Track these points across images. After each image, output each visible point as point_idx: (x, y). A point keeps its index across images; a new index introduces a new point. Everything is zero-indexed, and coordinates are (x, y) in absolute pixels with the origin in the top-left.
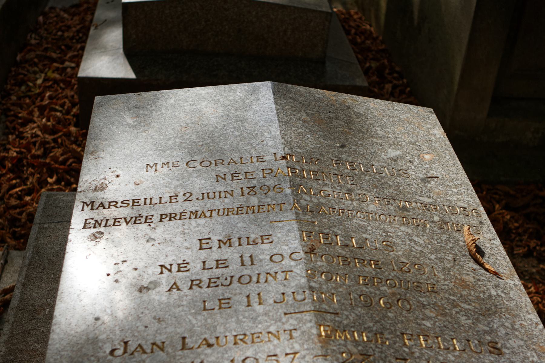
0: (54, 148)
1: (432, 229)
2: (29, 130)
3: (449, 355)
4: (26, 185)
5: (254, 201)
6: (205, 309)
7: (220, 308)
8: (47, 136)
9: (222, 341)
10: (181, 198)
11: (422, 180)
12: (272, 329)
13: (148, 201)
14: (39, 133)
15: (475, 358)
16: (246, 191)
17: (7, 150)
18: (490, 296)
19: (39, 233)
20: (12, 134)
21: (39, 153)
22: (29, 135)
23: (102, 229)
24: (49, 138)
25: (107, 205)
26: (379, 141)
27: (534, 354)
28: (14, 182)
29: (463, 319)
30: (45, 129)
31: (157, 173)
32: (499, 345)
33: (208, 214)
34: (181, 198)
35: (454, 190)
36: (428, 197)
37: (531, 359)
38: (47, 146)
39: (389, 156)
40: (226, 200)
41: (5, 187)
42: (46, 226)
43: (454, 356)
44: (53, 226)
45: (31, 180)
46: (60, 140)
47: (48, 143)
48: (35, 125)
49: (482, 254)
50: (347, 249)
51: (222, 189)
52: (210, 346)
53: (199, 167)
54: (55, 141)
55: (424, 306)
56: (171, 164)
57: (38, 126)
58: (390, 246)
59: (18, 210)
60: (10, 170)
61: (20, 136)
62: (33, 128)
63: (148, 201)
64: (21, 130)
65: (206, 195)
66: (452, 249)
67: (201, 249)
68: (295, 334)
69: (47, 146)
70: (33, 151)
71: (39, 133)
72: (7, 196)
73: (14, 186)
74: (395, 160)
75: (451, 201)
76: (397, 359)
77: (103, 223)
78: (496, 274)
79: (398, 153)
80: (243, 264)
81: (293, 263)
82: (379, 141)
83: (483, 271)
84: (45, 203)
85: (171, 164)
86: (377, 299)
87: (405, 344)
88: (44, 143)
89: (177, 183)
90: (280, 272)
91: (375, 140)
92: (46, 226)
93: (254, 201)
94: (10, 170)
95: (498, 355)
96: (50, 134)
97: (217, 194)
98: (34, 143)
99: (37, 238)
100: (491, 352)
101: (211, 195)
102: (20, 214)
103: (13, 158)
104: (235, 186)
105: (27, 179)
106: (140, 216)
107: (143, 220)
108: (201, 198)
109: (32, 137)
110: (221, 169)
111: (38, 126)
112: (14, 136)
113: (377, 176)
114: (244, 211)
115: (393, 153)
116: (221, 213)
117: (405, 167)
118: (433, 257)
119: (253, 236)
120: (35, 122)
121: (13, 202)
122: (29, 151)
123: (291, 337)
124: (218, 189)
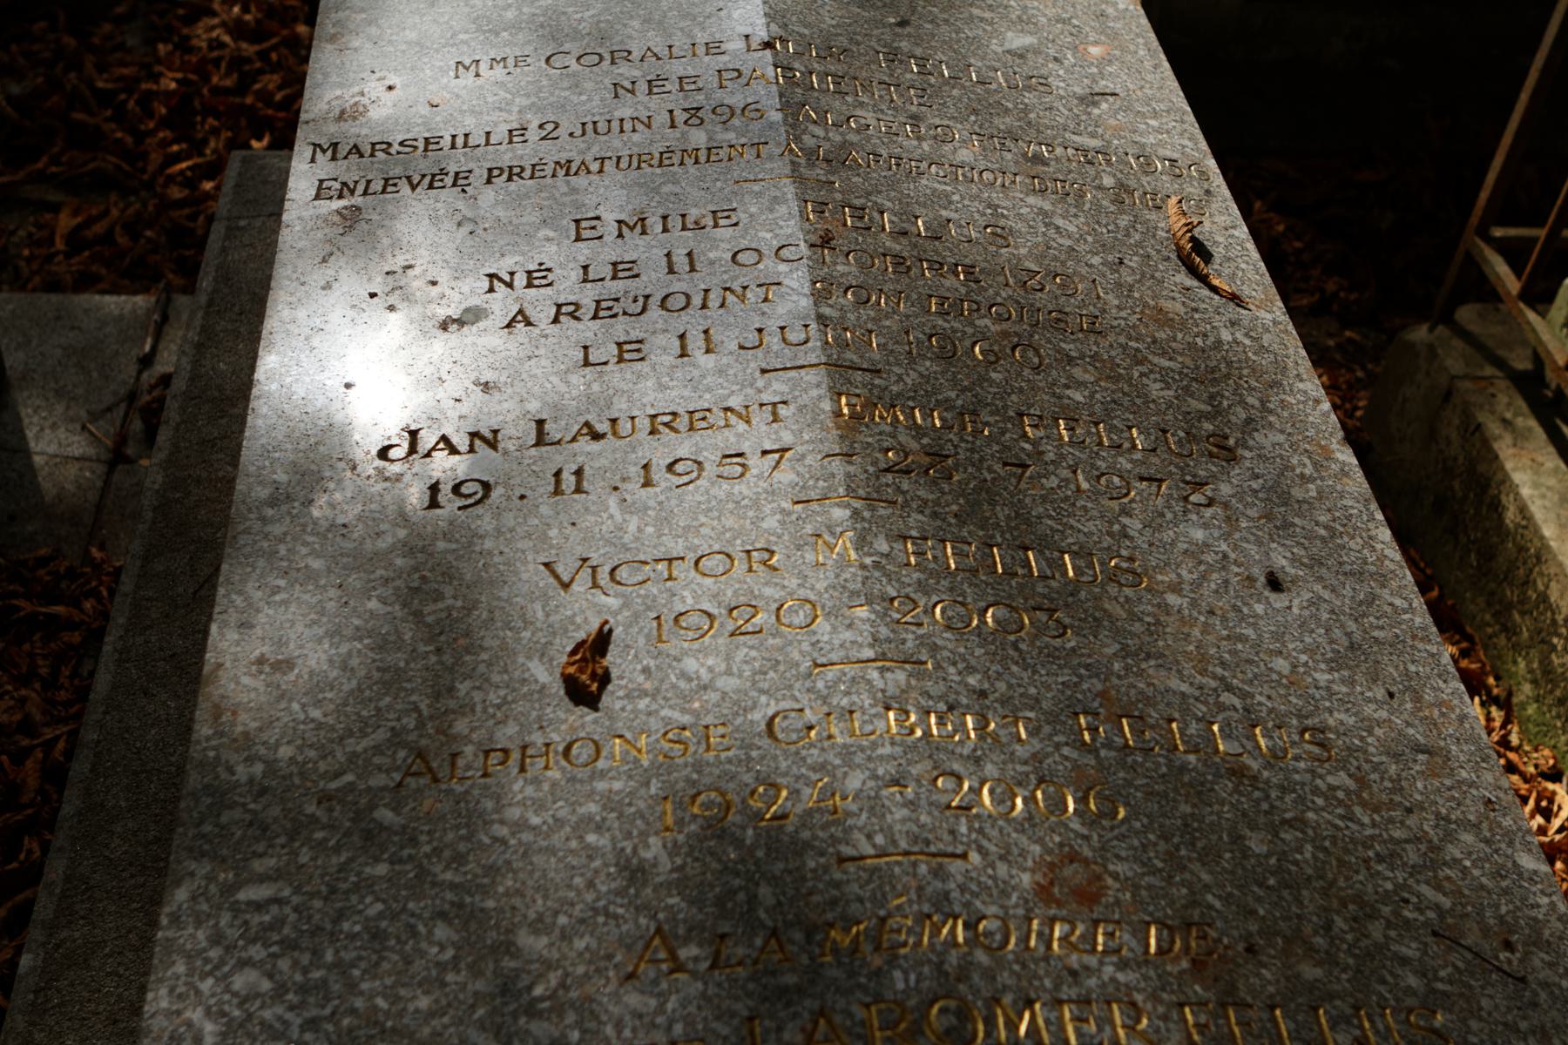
0: (261, 72)
1: (1096, 203)
2: (204, 33)
3: (1120, 459)
4: (201, 154)
5: (698, 138)
6: (587, 363)
7: (621, 360)
8: (244, 45)
9: (625, 427)
10: (533, 134)
11: (1082, 99)
12: (733, 402)
13: (460, 141)
14: (227, 39)
15: (1177, 466)
16: (680, 117)
17: (156, 78)
18: (1219, 343)
19: (227, 237)
20: (166, 41)
21: (228, 83)
22: (204, 45)
23: (357, 200)
24: (249, 49)
25: (367, 150)
26: (988, 15)
27: (1307, 461)
28: (175, 148)
29: (1155, 389)
30: (238, 30)
31: (480, 81)
32: (1231, 442)
33: (595, 167)
34: (533, 134)
35: (1153, 122)
36: (1093, 135)
37: (1298, 471)
38: (247, 68)
39: (1007, 46)
40: (636, 137)
41: (156, 158)
42: (242, 223)
43: (1131, 461)
44: (258, 223)
45: (212, 144)
46: (274, 56)
47: (248, 60)
48: (216, 21)
49: (1207, 257)
50: (904, 241)
51: (627, 113)
52: (597, 436)
53: (574, 66)
54: (263, 55)
55: (1070, 360)
56: (510, 61)
57: (224, 24)
58: (1002, 236)
59: (186, 211)
60: (164, 123)
61: (184, 46)
62: (213, 28)
63: (460, 141)
64: (185, 31)
65: (589, 127)
66: (1139, 245)
67: (578, 239)
68: (783, 411)
69: (247, 68)
70: (215, 80)
71: (227, 39)
72: (161, 180)
73: (178, 158)
74: (1021, 56)
75: (1143, 146)
76: (1005, 464)
77: (360, 188)
78: (1235, 298)
79: (1028, 40)
80: (671, 271)
81: (783, 267)
82: (988, 15)
83: (1206, 292)
84: (240, 174)
85: (510, 61)
86: (968, 343)
87: (1025, 435)
88: (237, 62)
89: (525, 102)
90: (753, 287)
91: (976, 11)
92: (242, 223)
93: (698, 138)
94: (164, 123)
95: (1228, 461)
96: (252, 41)
97: (615, 125)
98: (217, 62)
99: (224, 250)
100: (1211, 455)
101: (602, 127)
102: (193, 217)
103: (169, 94)
104: (657, 106)
105: (205, 142)
106: (445, 173)
107: (449, 180)
108: (578, 132)
109: (211, 48)
110: (625, 71)
111: (224, 24)
112: (170, 47)
113: (979, 89)
114: (676, 159)
115: (1017, 41)
116: (623, 164)
117: (1044, 72)
118: (1096, 260)
119: (694, 213)
120: (214, 14)
121: (176, 193)
122: (206, 78)
123: (776, 418)
124: (618, 114)
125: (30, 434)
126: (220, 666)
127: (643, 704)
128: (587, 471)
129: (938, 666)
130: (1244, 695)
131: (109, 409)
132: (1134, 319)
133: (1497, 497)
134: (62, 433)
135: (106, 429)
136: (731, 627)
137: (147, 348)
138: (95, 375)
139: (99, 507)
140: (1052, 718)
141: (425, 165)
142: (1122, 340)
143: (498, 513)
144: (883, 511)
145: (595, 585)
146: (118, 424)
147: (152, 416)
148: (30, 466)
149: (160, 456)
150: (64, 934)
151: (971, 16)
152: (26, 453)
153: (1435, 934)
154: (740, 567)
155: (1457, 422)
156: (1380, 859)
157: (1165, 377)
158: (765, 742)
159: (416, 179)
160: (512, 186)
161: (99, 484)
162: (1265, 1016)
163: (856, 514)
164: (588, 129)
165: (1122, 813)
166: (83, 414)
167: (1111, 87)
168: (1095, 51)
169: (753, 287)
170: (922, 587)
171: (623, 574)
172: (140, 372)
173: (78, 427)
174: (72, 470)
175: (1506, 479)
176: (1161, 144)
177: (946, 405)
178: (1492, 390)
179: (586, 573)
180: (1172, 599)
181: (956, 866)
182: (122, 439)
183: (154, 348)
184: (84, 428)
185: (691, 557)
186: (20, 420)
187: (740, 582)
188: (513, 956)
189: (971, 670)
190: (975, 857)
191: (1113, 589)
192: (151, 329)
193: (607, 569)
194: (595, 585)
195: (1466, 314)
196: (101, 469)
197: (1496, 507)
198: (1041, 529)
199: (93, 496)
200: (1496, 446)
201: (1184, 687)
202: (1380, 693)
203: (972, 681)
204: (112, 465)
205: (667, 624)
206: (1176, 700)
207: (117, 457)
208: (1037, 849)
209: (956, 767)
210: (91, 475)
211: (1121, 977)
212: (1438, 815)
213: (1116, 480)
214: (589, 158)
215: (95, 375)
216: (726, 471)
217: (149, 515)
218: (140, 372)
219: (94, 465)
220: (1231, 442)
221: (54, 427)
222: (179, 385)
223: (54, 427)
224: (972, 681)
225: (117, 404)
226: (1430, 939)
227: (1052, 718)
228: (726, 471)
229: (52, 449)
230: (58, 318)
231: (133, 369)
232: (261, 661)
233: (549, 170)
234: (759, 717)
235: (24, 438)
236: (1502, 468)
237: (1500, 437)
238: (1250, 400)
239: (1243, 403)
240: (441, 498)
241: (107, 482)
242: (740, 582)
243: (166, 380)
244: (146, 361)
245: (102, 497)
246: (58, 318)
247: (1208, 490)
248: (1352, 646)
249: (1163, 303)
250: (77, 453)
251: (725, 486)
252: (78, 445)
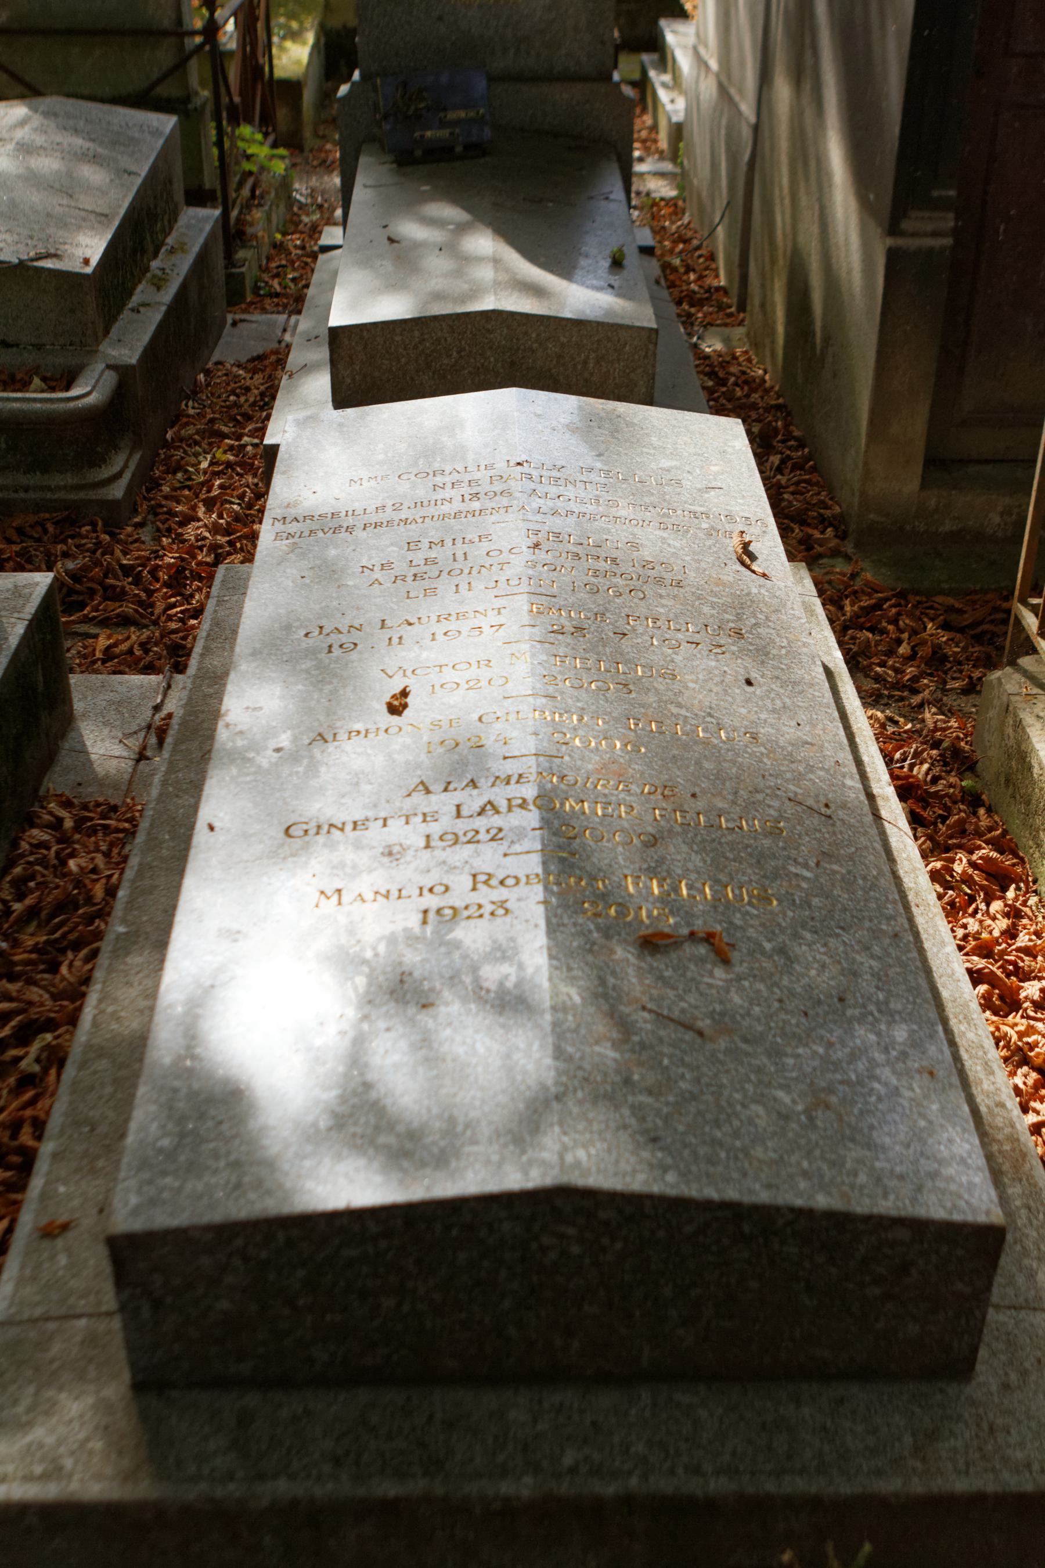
0: (229, 554)
1: (695, 535)
2: (190, 532)
4: (189, 604)
5: (476, 505)
6: (408, 598)
7: (425, 595)
8: (219, 537)
9: (424, 620)
10: (389, 509)
11: (699, 490)
12: (481, 609)
13: (350, 513)
14: (207, 534)
16: (467, 497)
17: (161, 558)
18: (749, 594)
19: (217, 605)
20: (167, 537)
21: (208, 560)
22: (192, 538)
23: (296, 539)
24: (222, 539)
25: (301, 519)
26: (652, 451)
28: (173, 600)
29: (706, 609)
30: (215, 529)
31: (361, 487)
32: (743, 631)
33: (420, 520)
34: (389, 509)
35: (741, 501)
36: (701, 506)
38: (220, 551)
39: (660, 465)
40: (442, 507)
41: (160, 606)
42: (226, 598)
44: (235, 598)
45: (197, 597)
46: (238, 545)
47: (221, 546)
48: (200, 523)
49: (753, 557)
50: (580, 547)
51: (439, 497)
52: (410, 624)
53: (413, 478)
54: (231, 543)
55: (661, 596)
56: (379, 478)
57: (205, 526)
58: (635, 546)
59: (181, 634)
60: (166, 584)
61: (180, 539)
62: (198, 528)
63: (350, 513)
64: (180, 531)
65: (419, 504)
66: (716, 552)
67: (409, 550)
68: (502, 611)
69: (220, 551)
70: (200, 558)
71: (207, 534)
72: (163, 619)
73: (174, 606)
74: (668, 470)
75: (731, 511)
77: (298, 535)
78: (764, 575)
79: (674, 463)
80: (455, 560)
81: (513, 556)
82: (652, 451)
83: (750, 573)
84: (224, 576)
85: (379, 478)
86: (606, 588)
87: (628, 623)
88: (214, 548)
89: (386, 495)
90: (496, 565)
91: (645, 450)
92: (226, 598)
93: (476, 505)
94: (166, 584)
96: (223, 536)
97: (433, 503)
98: (201, 548)
99: (215, 611)
101: (425, 504)
102: (184, 638)
103: (170, 565)
104: (455, 494)
105: (192, 596)
106: (340, 526)
107: (343, 530)
108: (413, 506)
109: (197, 541)
110: (439, 480)
111: (205, 526)
112: (170, 540)
113: (639, 485)
114: (463, 515)
115: (666, 463)
116: (435, 519)
117: (680, 478)
118: (688, 558)
119: (469, 537)
120: (199, 520)
121: (173, 625)
122: (194, 557)
123: (499, 613)
124: (435, 498)
125: (88, 743)
126: (228, 710)
127: (422, 714)
128: (404, 637)
129: (563, 699)
130: (718, 719)
131: (135, 733)
132: (703, 582)
133: (1030, 762)
134: (107, 744)
135: (135, 743)
136: (467, 686)
137: (159, 701)
138: (126, 715)
139: (130, 782)
140: (617, 720)
141: (334, 524)
142: (693, 590)
143: (361, 653)
144: (547, 645)
145: (405, 675)
146: (141, 740)
147: (161, 733)
148: (89, 760)
149: (166, 754)
150: (139, 884)
151: (642, 452)
152: (86, 753)
153: (790, 800)
154: (475, 665)
155: (1011, 722)
156: (771, 775)
157: (713, 606)
158: (479, 723)
159: (326, 530)
160: (376, 531)
161: (130, 770)
162: (695, 815)
163: (533, 646)
164: (418, 504)
165: (643, 750)
166: (120, 735)
167: (719, 485)
168: (714, 469)
169: (496, 565)
170: (560, 672)
171: (417, 672)
172: (154, 715)
173: (117, 741)
174: (115, 762)
175: (1033, 749)
176: (743, 510)
177: (590, 610)
178: (1035, 701)
179: (401, 672)
180: (691, 685)
181: (557, 761)
182: (144, 748)
183: (162, 701)
184: (121, 741)
185: (451, 665)
186: (82, 736)
187: (473, 672)
188: (387, 1147)
189: (578, 700)
190: (567, 758)
191: (661, 680)
192: (161, 689)
193: (411, 670)
194: (405, 675)
195: (1026, 661)
196: (131, 763)
197: (1030, 768)
198: (627, 657)
199: (127, 776)
200: (1028, 730)
201: (688, 714)
202: (793, 723)
203: (579, 704)
204: (138, 761)
205: (437, 687)
206: (682, 718)
207: (141, 757)
208: (598, 758)
209: (564, 730)
210: (127, 766)
211: (628, 798)
212: (808, 765)
213: (674, 642)
214: (417, 517)
215: (126, 715)
216: (471, 634)
217: (177, 727)
218: (154, 715)
219: (127, 761)
220: (743, 631)
221: (102, 740)
222: (175, 721)
223: (102, 740)
224: (579, 704)
225: (140, 730)
226: (787, 801)
227: (617, 720)
228: (471, 634)
229: (101, 752)
230: (103, 686)
231: (149, 713)
232: (247, 708)
233: (396, 523)
234: (476, 717)
235: (85, 745)
236: (1031, 743)
237: (1033, 725)
238: (760, 616)
239: (755, 617)
240: (333, 650)
241: (135, 770)
242: (473, 672)
243: (170, 716)
244: (157, 708)
245: (132, 777)
246: (103, 686)
247: (724, 649)
248: (784, 707)
249: (721, 576)
250: (117, 754)
251: (471, 639)
252: (118, 750)
